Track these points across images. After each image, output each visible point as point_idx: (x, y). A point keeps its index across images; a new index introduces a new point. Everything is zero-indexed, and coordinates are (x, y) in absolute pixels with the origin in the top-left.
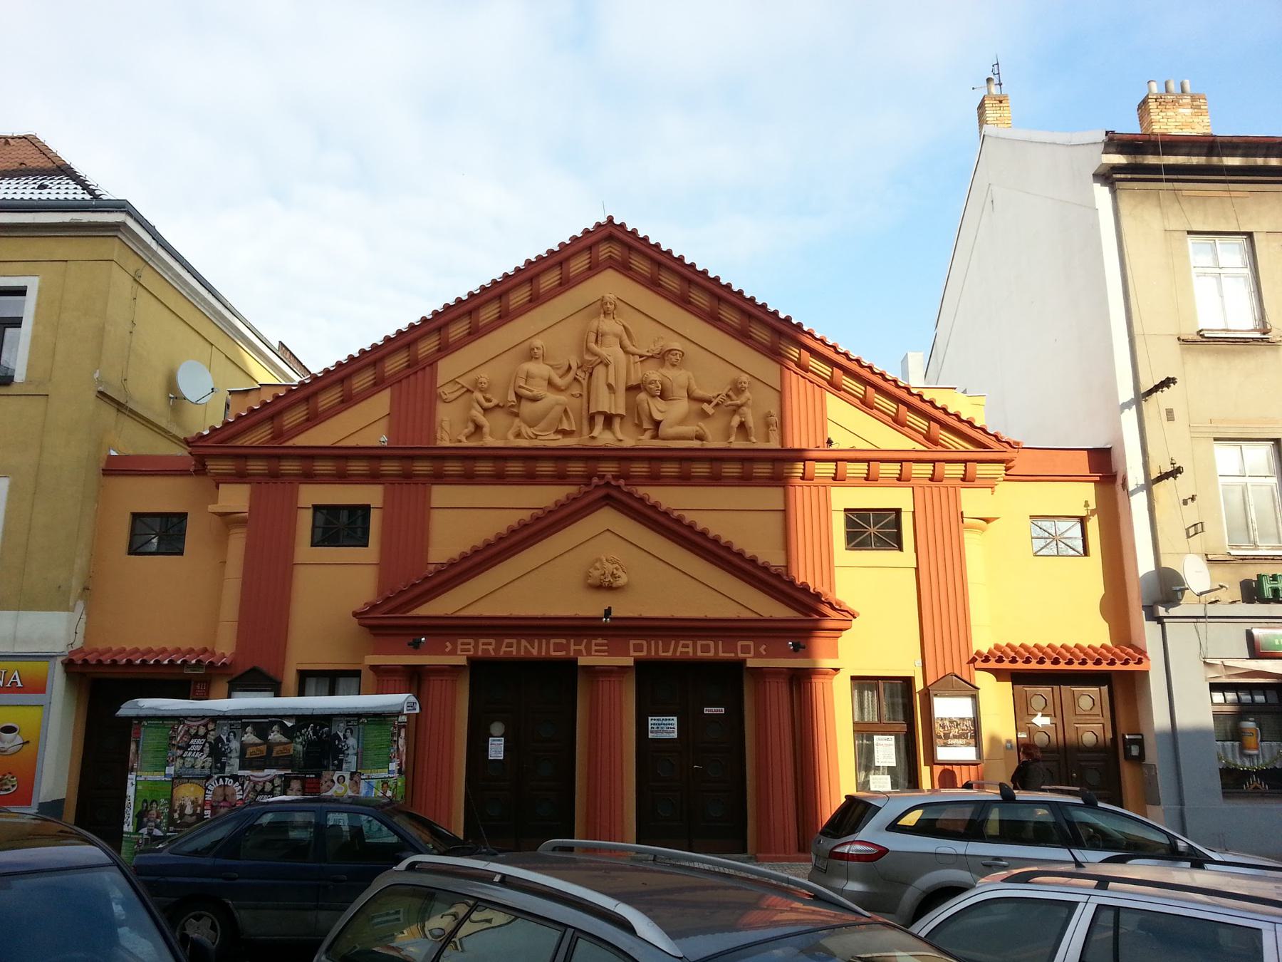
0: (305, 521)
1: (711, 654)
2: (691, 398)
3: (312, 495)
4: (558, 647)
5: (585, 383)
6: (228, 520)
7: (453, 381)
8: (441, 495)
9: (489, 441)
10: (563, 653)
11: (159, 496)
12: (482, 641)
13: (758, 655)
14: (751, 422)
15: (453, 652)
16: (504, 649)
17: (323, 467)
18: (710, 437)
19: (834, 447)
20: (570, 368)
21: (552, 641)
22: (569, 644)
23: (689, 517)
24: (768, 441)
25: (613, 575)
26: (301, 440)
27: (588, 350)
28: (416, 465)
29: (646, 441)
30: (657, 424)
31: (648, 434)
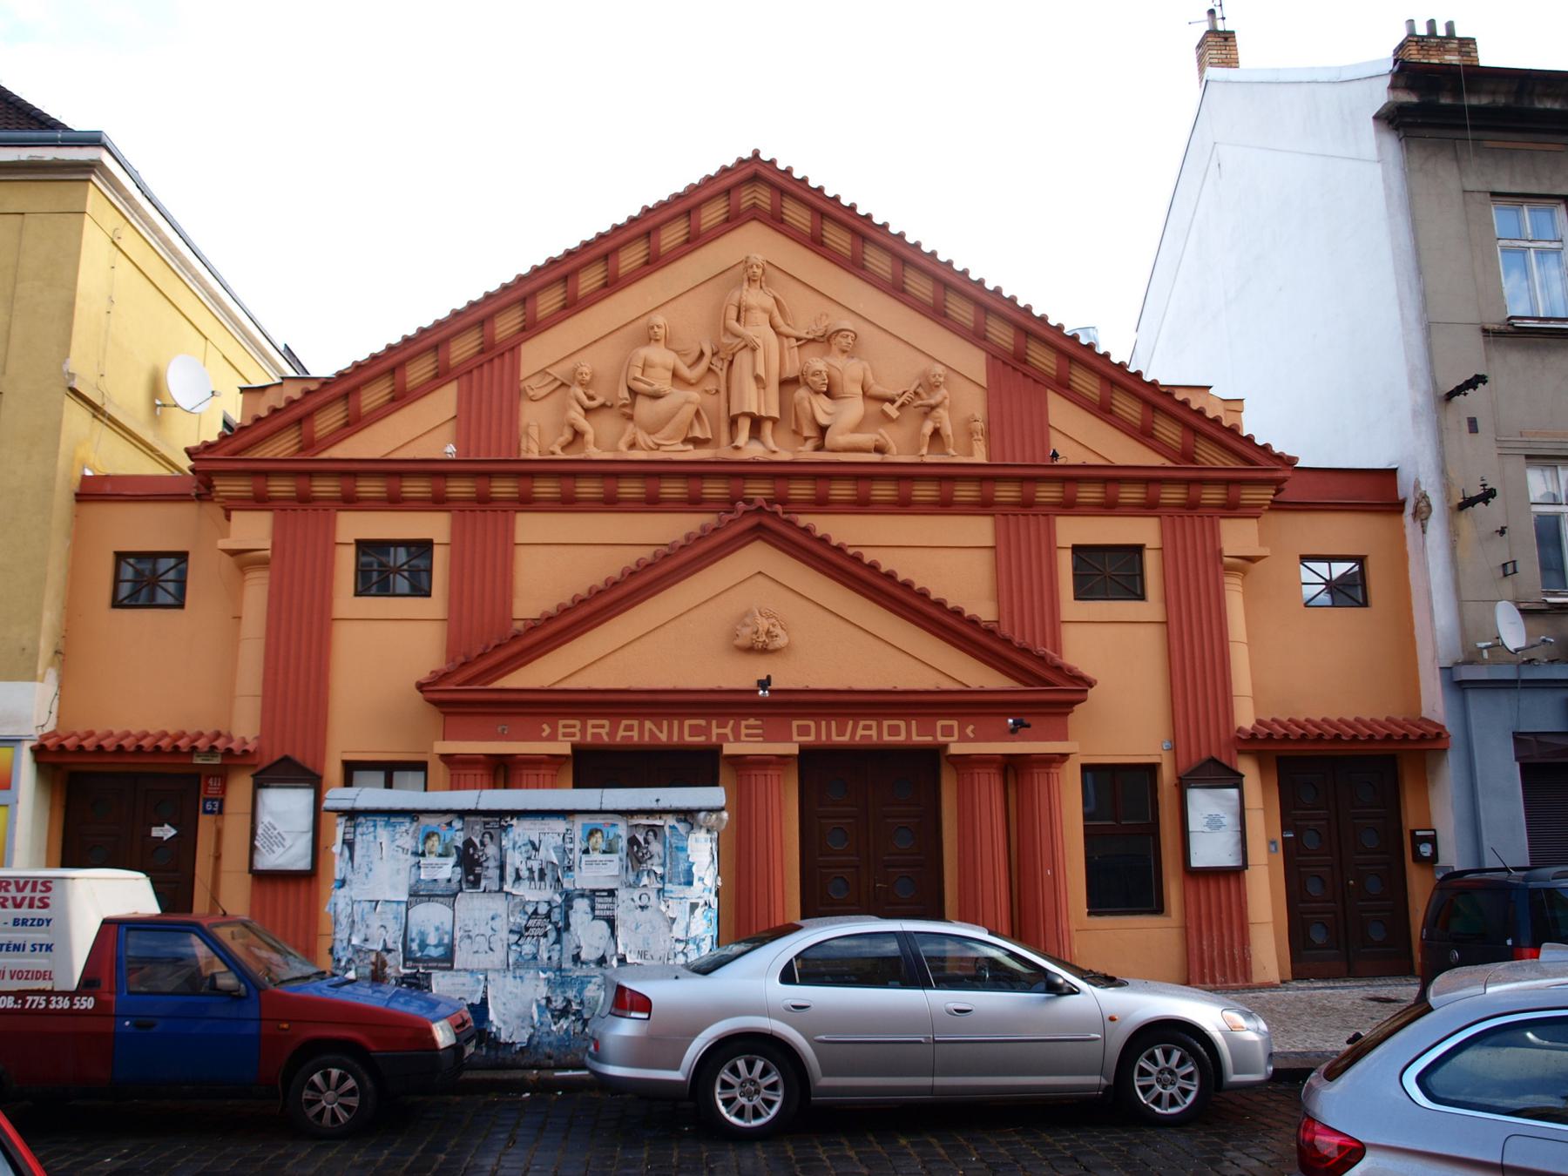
0: (346, 563)
1: (902, 738)
2: (867, 396)
4: (694, 731)
5: (723, 375)
6: (242, 558)
7: (543, 372)
8: (528, 526)
9: (594, 453)
10: (701, 739)
11: (148, 529)
12: (590, 722)
13: (963, 738)
14: (947, 429)
15: (553, 737)
16: (621, 733)
17: (370, 488)
18: (894, 449)
19: (1060, 462)
20: (702, 354)
21: (687, 723)
22: (709, 724)
23: (869, 556)
24: (971, 454)
25: (768, 632)
26: (338, 452)
27: (726, 329)
28: (494, 485)
29: (807, 453)
30: (823, 430)
31: (810, 445)
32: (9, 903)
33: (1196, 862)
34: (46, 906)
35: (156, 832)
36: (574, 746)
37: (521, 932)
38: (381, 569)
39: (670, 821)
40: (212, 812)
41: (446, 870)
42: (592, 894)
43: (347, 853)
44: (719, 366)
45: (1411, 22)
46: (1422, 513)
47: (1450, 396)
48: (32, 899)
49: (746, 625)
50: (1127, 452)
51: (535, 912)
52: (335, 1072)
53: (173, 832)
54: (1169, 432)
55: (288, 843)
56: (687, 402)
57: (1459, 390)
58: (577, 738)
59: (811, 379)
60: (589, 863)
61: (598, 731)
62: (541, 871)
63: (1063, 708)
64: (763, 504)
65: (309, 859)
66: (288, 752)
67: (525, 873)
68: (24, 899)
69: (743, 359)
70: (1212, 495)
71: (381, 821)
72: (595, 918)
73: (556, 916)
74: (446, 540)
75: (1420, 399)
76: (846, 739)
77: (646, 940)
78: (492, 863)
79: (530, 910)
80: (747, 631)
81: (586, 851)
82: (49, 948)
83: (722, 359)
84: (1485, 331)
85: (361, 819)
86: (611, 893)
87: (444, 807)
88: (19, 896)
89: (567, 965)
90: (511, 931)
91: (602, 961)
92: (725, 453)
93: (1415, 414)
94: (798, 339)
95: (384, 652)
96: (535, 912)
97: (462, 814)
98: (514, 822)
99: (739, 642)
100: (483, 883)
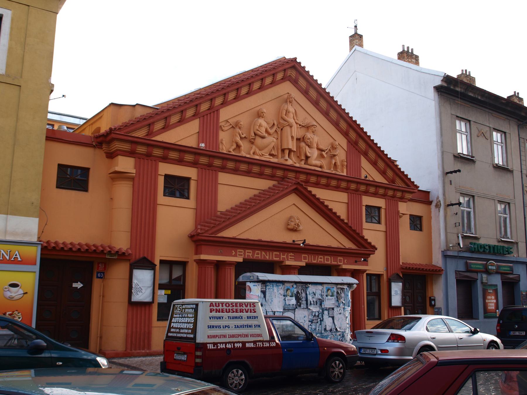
0: (161, 181)
1: (329, 262)
2: (318, 149)
3: (166, 169)
4: (276, 256)
5: (279, 133)
6: (118, 176)
7: (227, 121)
8: (223, 178)
9: (243, 154)
10: (278, 259)
11: (74, 156)
12: (247, 251)
13: (344, 264)
14: (339, 163)
15: (235, 256)
16: (256, 255)
17: (173, 155)
18: (325, 168)
19: (367, 179)
20: (274, 124)
21: (274, 253)
22: (280, 254)
23: (326, 203)
24: (343, 172)
25: (298, 224)
26: (159, 138)
27: (282, 118)
28: (212, 161)
29: (302, 165)
30: (307, 158)
31: (303, 162)
32: (244, 311)
33: (393, 305)
34: (255, 312)
35: (75, 285)
36: (243, 259)
37: (312, 321)
38: (177, 187)
39: (345, 287)
40: (100, 278)
41: (293, 301)
42: (328, 309)
43: (262, 296)
44: (279, 131)
45: (403, 46)
46: (438, 206)
47: (447, 173)
48: (251, 309)
49: (292, 221)
50: (379, 178)
51: (315, 315)
52: (337, 362)
53: (82, 285)
54: (390, 173)
55: (143, 291)
56: (273, 141)
57: (451, 172)
58: (307, 261)
59: (306, 140)
60: (328, 299)
61: (249, 254)
62: (316, 301)
63: (366, 256)
64: (296, 181)
65: (151, 297)
66: (146, 256)
67: (312, 303)
68: (248, 309)
69: (287, 129)
70: (399, 194)
71: (275, 284)
72: (329, 317)
73: (320, 316)
74: (196, 179)
75: (440, 173)
76: (315, 261)
77: (341, 323)
78: (304, 299)
79: (314, 314)
80: (293, 224)
81: (327, 296)
82: (259, 326)
83: (281, 125)
84: (454, 156)
85: (268, 284)
86: (333, 309)
87: (293, 280)
88: (247, 308)
89: (323, 332)
90: (309, 321)
91: (331, 330)
92: (282, 161)
93: (439, 176)
94: (300, 125)
95: (175, 219)
96: (315, 315)
97: (296, 283)
98: (310, 286)
99: (289, 227)
100: (302, 305)
